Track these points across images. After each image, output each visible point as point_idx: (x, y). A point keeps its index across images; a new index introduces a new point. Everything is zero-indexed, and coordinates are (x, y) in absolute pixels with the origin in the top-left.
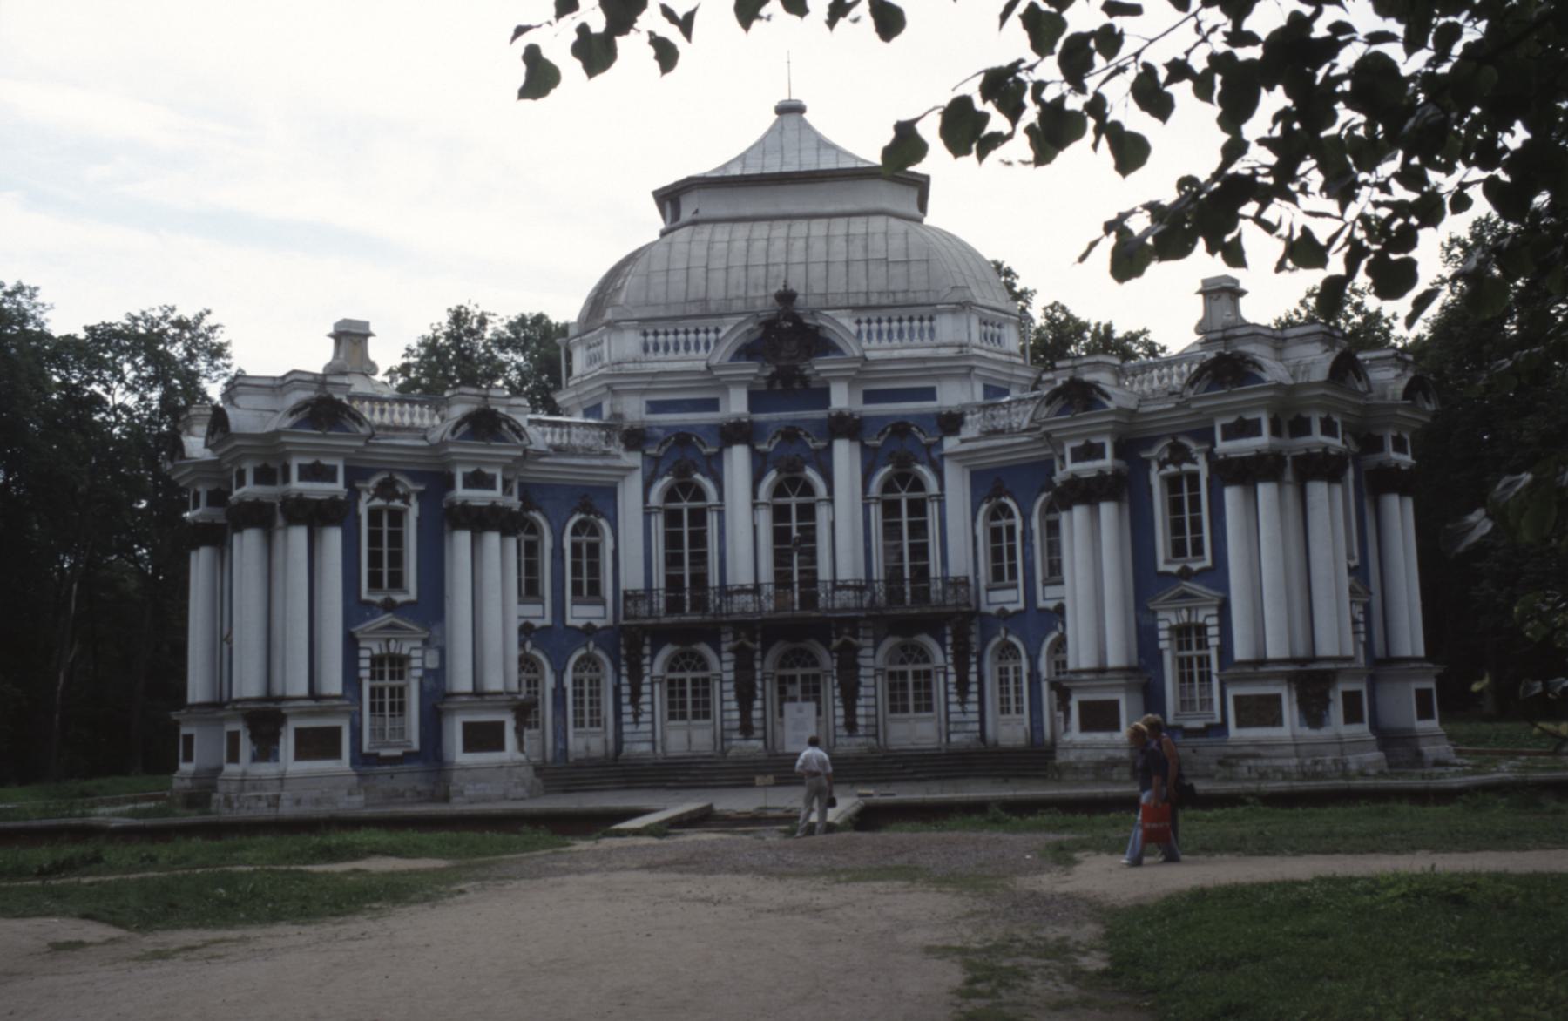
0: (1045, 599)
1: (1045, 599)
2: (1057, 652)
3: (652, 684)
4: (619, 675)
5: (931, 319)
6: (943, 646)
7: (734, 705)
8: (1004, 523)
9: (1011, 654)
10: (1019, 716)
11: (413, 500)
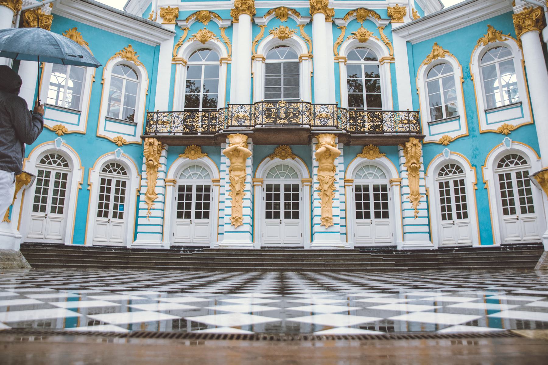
0: (488, 124)
1: (488, 124)
2: (500, 166)
3: (165, 187)
7: (228, 203)
10: (463, 220)
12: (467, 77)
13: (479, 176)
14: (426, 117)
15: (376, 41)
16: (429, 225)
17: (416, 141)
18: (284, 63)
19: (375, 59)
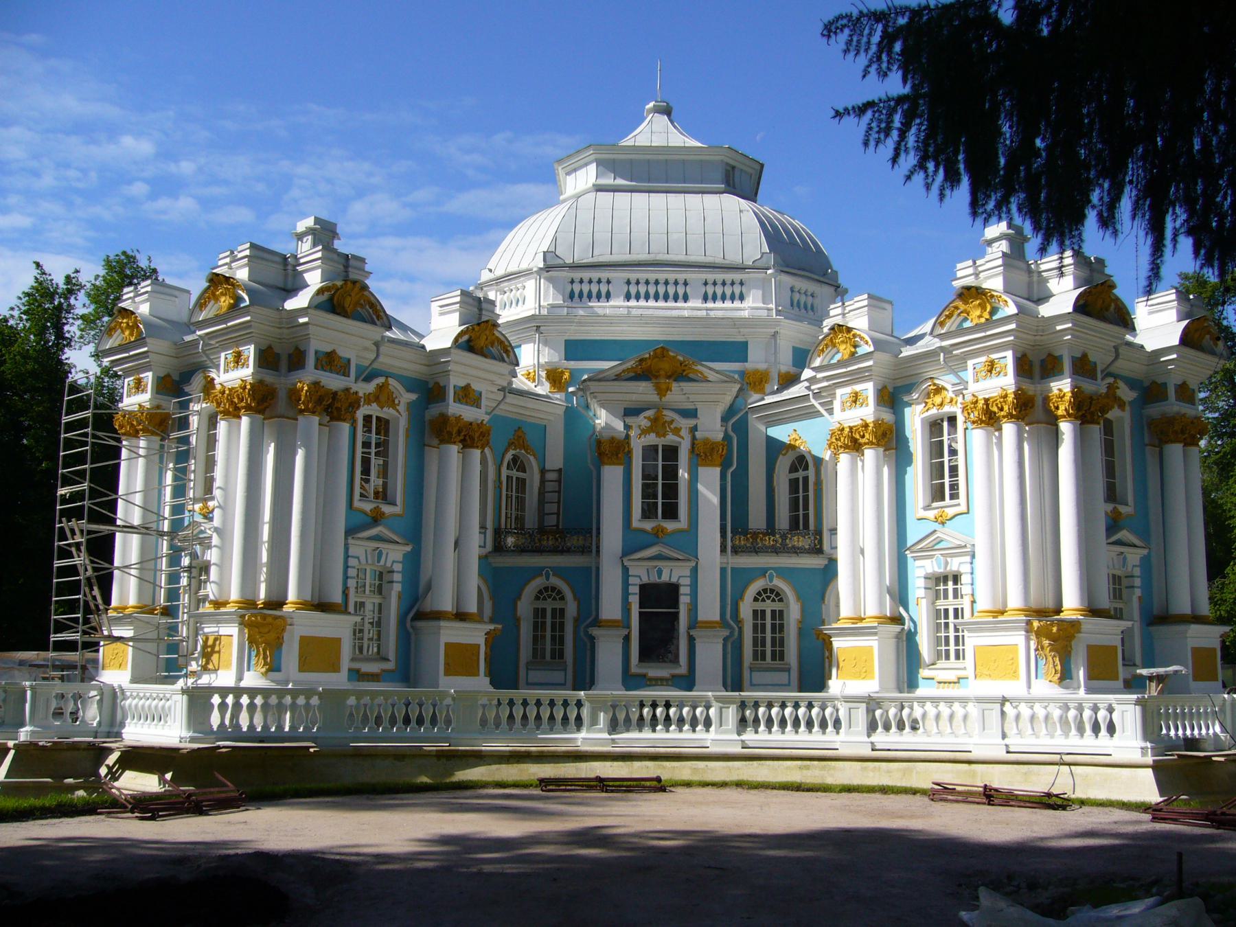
11: (402, 408)
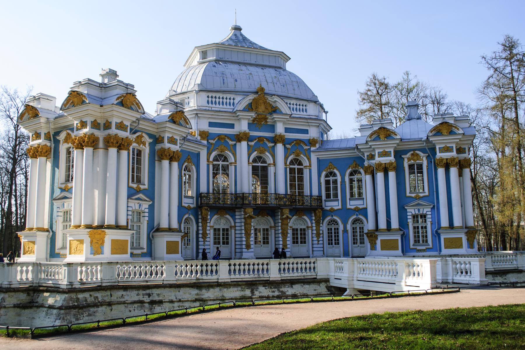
2: (353, 224)
4: (198, 226)
5: (306, 106)
6: (311, 220)
7: (244, 239)
8: (331, 178)
9: (333, 224)
12: (343, 181)
13: (345, 227)
14: (324, 198)
15: (303, 157)
16: (323, 247)
17: (320, 210)
18: (261, 166)
19: (302, 165)
